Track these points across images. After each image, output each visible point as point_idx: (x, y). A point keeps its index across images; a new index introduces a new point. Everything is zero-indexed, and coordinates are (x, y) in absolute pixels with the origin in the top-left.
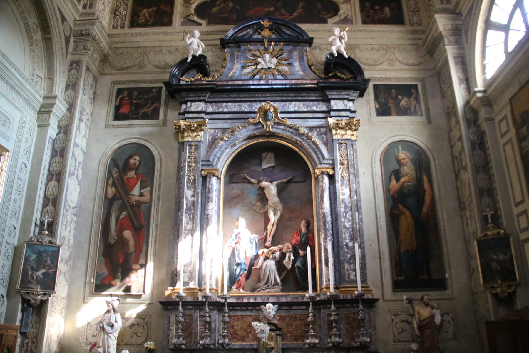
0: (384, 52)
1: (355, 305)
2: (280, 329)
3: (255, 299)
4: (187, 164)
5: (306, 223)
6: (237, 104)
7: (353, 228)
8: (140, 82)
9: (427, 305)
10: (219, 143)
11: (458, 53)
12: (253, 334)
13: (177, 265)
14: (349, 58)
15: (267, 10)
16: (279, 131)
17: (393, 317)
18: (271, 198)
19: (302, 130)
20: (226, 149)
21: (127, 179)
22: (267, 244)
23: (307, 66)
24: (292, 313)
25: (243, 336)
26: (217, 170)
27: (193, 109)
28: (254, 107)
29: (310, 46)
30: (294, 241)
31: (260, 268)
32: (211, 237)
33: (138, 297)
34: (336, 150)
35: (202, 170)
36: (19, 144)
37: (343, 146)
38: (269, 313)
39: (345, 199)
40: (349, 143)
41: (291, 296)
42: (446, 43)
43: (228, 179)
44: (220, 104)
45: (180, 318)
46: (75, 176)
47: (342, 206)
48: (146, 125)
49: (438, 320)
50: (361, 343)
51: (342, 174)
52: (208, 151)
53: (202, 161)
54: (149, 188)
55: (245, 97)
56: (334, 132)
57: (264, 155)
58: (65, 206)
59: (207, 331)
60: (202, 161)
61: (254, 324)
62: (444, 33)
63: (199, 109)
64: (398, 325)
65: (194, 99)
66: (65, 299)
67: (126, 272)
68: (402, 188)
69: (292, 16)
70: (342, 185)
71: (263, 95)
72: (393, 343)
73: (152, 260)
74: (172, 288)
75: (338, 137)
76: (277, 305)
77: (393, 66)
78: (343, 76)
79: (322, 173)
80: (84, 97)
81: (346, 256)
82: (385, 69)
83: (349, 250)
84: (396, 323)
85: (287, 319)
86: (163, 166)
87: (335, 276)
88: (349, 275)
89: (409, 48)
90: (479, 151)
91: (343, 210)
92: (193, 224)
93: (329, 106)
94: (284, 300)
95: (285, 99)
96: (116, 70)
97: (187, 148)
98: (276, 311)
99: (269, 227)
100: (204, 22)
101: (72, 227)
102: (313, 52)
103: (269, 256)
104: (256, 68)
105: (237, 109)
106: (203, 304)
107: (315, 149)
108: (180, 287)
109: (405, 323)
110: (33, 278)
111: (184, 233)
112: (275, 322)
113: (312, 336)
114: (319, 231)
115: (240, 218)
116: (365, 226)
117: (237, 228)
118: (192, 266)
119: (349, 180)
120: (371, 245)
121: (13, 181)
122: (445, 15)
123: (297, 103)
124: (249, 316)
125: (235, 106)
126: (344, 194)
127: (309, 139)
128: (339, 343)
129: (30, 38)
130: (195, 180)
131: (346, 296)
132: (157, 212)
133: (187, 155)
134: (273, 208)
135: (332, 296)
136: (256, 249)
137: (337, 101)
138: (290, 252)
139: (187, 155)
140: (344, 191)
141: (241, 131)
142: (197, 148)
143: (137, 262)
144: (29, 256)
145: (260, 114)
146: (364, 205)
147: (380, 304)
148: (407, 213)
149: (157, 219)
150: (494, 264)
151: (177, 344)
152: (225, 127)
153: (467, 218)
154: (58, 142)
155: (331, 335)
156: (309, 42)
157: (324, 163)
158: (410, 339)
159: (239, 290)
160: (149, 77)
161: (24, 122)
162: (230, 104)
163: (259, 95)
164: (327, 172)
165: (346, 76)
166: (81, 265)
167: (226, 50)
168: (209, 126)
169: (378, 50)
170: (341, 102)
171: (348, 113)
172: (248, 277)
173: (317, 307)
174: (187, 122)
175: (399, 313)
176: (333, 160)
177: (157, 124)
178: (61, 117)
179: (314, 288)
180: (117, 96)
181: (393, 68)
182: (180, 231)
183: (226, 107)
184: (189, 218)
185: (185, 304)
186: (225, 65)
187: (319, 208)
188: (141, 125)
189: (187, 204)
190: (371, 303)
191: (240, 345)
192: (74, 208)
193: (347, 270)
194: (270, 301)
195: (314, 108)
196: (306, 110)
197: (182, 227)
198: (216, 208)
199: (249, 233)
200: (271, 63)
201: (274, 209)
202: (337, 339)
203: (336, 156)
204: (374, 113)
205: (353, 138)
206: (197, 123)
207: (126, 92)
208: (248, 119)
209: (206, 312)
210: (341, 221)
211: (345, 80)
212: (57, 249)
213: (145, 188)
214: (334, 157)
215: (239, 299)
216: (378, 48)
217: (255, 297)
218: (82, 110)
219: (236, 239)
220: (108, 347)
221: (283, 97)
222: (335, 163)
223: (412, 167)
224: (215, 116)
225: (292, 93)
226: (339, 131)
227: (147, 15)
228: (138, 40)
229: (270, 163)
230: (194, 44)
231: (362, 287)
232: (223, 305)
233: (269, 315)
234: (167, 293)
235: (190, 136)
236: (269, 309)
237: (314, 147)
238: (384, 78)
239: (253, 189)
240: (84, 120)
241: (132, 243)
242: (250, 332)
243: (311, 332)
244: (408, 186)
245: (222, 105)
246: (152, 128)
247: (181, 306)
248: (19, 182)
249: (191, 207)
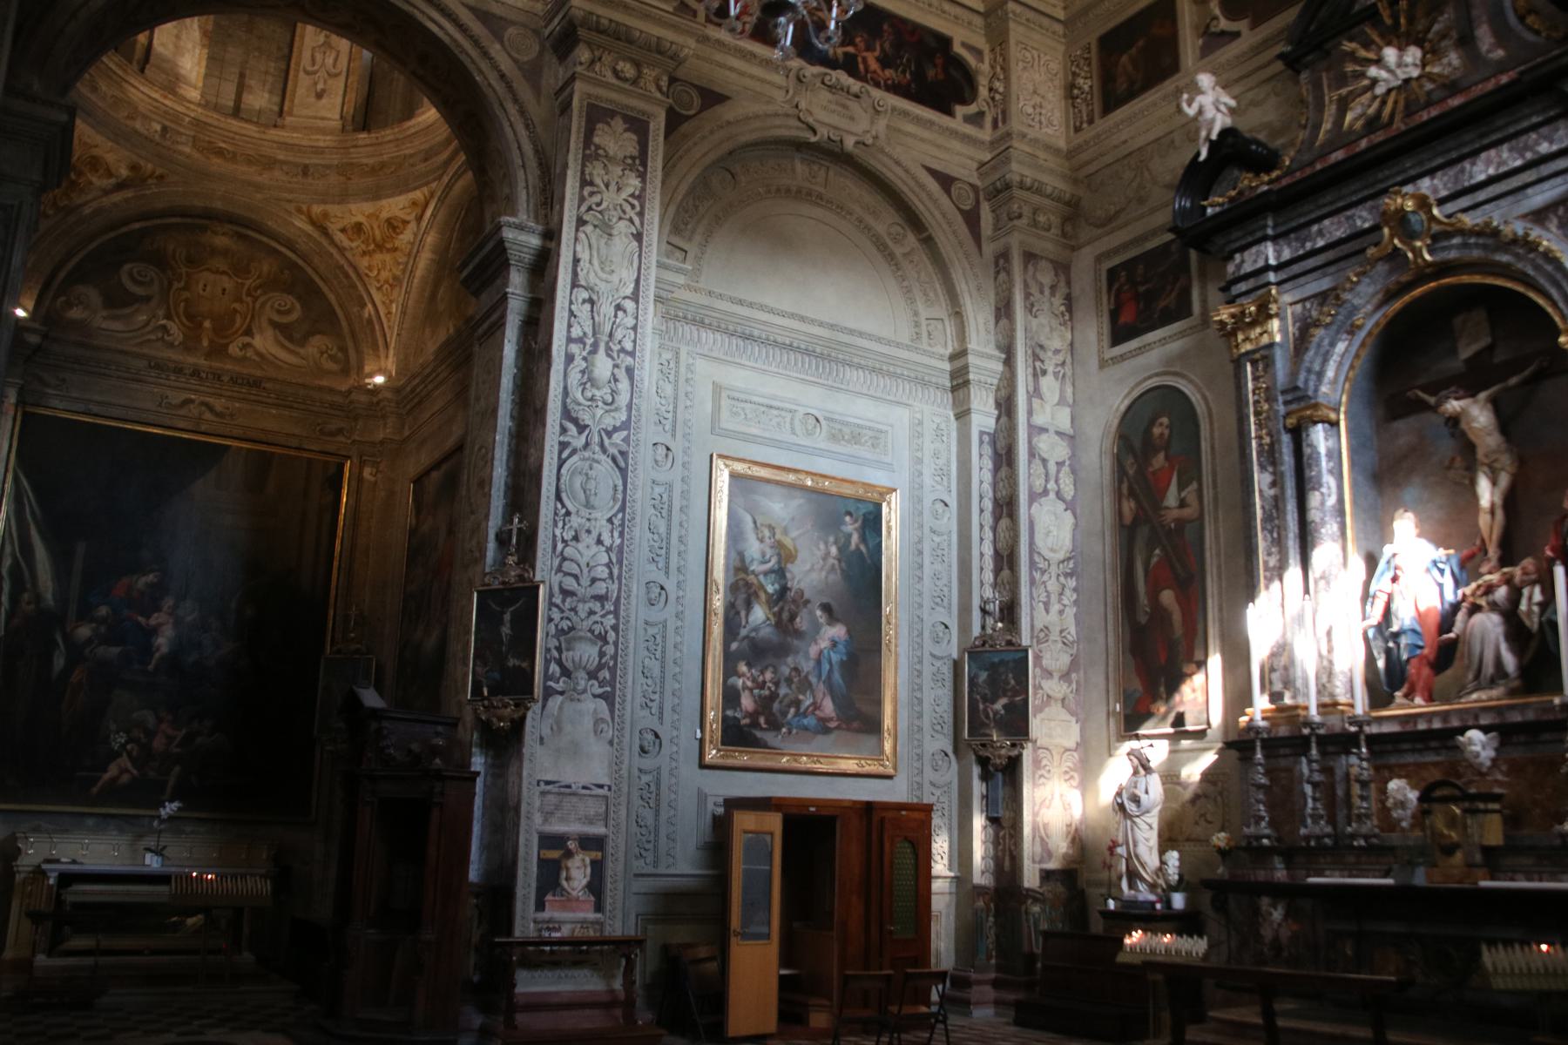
6: (1342, 217)
16: (1453, 255)
20: (1333, 344)
21: (1154, 473)
33: (1200, 734)
36: (919, 467)
38: (1477, 755)
44: (1304, 232)
46: (1052, 495)
54: (1194, 485)
55: (1355, 192)
58: (1032, 564)
60: (1284, 392)
65: (1243, 242)
66: (1075, 750)
67: (1174, 682)
73: (1218, 648)
80: (1035, 322)
92: (1280, 552)
94: (1516, 717)
95: (1454, 155)
96: (1098, 227)
98: (1496, 750)
100: (1242, 26)
101: (1066, 602)
107: (1554, 273)
110: (987, 716)
111: (1265, 577)
121: (920, 541)
123: (1493, 152)
125: (1339, 222)
129: (890, 257)
130: (1272, 445)
132: (1217, 537)
134: (1486, 469)
138: (1533, 583)
141: (1360, 288)
143: (1189, 658)
144: (976, 676)
149: (1218, 555)
154: (1001, 436)
159: (1412, 700)
161: (920, 423)
162: (1326, 222)
166: (1098, 678)
178: (995, 382)
183: (1320, 233)
185: (1323, 741)
188: (1163, 341)
189: (1263, 507)
192: (1063, 562)
195: (1544, 148)
196: (1518, 163)
200: (1406, 66)
207: (1123, 274)
208: (1363, 251)
212: (1020, 655)
213: (1187, 486)
217: (1445, 716)
218: (1038, 350)
219: (1388, 569)
220: (1135, 845)
221: (1449, 151)
224: (1296, 269)
227: (1130, 68)
228: (1123, 138)
237: (1549, 268)
240: (1050, 369)
241: (1177, 617)
246: (1184, 340)
247: (1259, 749)
248: (937, 539)
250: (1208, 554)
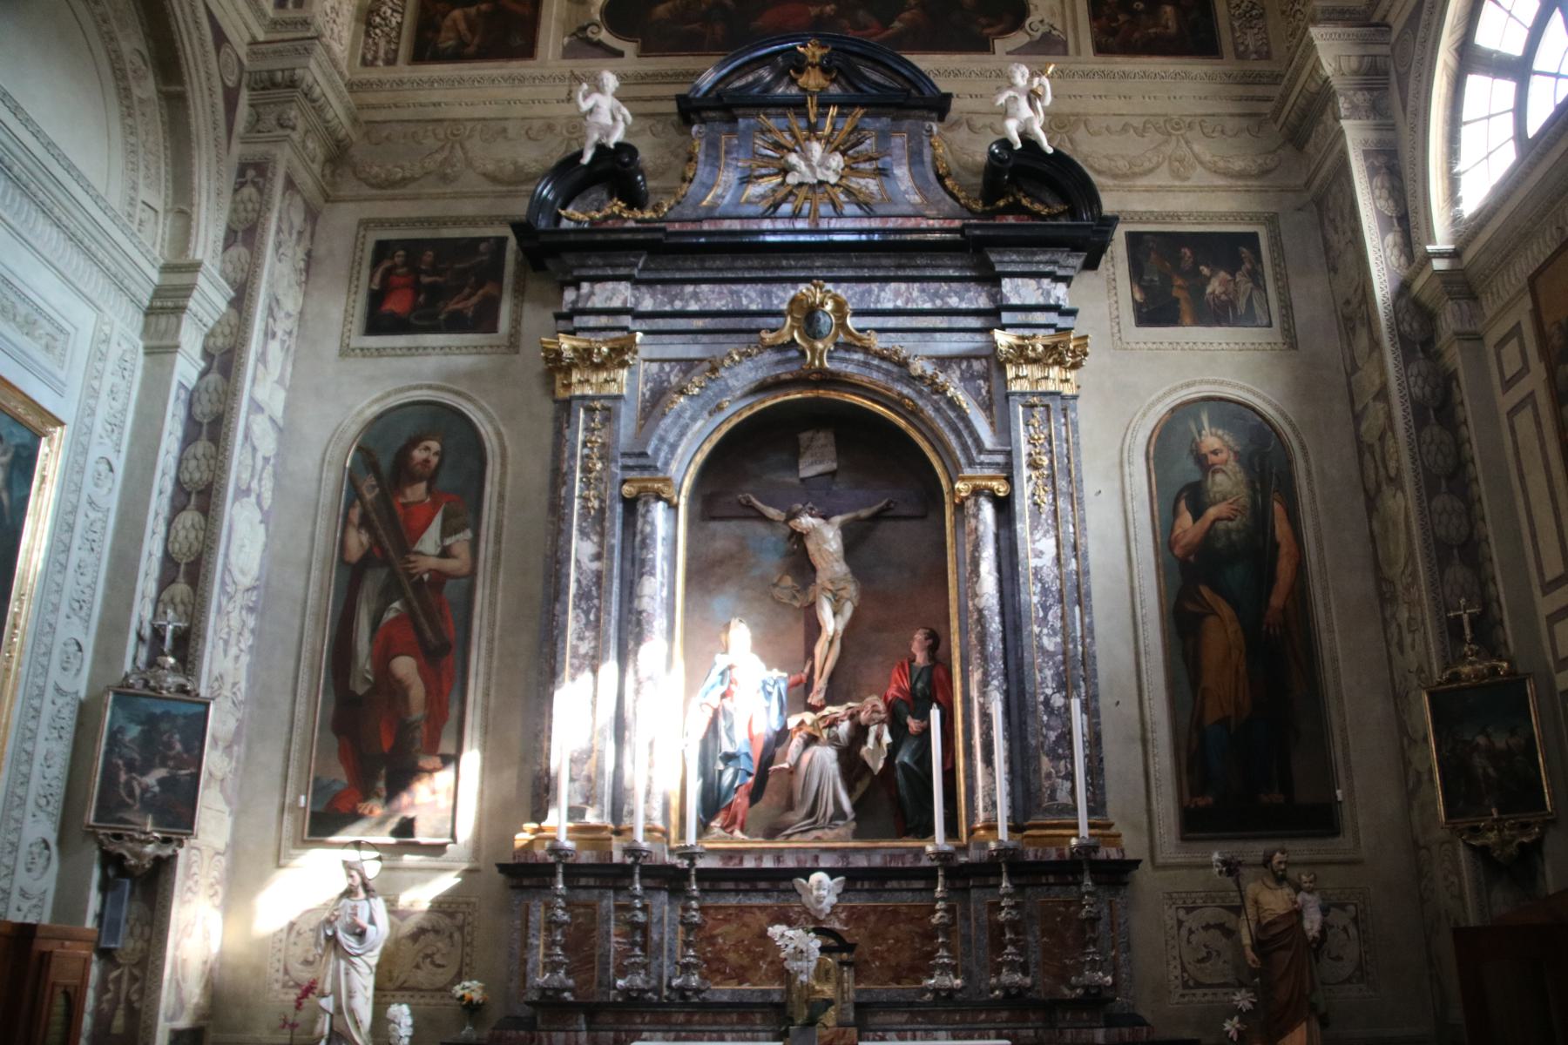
0: (1159, 137)
1: (1070, 878)
2: (850, 948)
3: (778, 859)
4: (579, 463)
5: (926, 639)
6: (725, 288)
7: (1064, 653)
8: (442, 222)
9: (1281, 879)
10: (672, 402)
11: (1380, 142)
12: (772, 962)
13: (548, 758)
15: (814, 11)
17: (1182, 913)
18: (824, 565)
19: (919, 366)
20: (694, 419)
21: (405, 506)
22: (814, 699)
23: (932, 176)
24: (886, 901)
25: (742, 967)
26: (666, 481)
27: (597, 302)
28: (777, 297)
29: (941, 119)
30: (892, 692)
31: (793, 770)
32: (650, 678)
33: (437, 850)
34: (1018, 425)
35: (624, 482)
36: (92, 402)
37: (1038, 413)
38: (819, 900)
39: (1041, 568)
40: (1055, 405)
41: (883, 851)
42: (1343, 112)
43: (698, 507)
44: (675, 289)
45: (560, 912)
46: (253, 499)
47: (1033, 589)
48: (458, 348)
49: (1312, 922)
50: (1087, 988)
51: (1034, 495)
52: (641, 427)
53: (624, 455)
54: (468, 534)
55: (750, 269)
56: (1011, 372)
57: (804, 437)
58: (223, 583)
59: (637, 951)
60: (624, 455)
61: (776, 931)
62: (1336, 83)
63: (616, 303)
64: (1194, 938)
65: (600, 272)
66: (223, 854)
67: (402, 777)
68: (1209, 535)
69: (890, 31)
70: (1033, 528)
71: (802, 263)
72: (1181, 991)
73: (476, 743)
74: (535, 826)
75: (1024, 386)
76: (841, 878)
77: (1188, 178)
78: (1037, 207)
79: (977, 492)
80: (278, 265)
81: (1046, 737)
82: (1160, 189)
83: (1054, 718)
84: (1191, 932)
85: (872, 918)
86: (509, 468)
87: (1012, 794)
88: (1053, 791)
89: (1231, 124)
90: (1436, 429)
91: (1035, 599)
92: (597, 638)
93: (997, 295)
94: (861, 862)
95: (866, 273)
96: (372, 186)
97: (578, 417)
98: (838, 895)
99: (820, 649)
100: (629, 48)
101: (243, 646)
102: (949, 135)
103: (818, 734)
104: (783, 183)
105: (727, 304)
106: (624, 871)
108: (557, 821)
109: (1218, 933)
110: (131, 794)
111: (572, 665)
112: (837, 926)
113: (945, 969)
114: (965, 661)
115: (735, 622)
116: (1099, 649)
117: (726, 651)
118: (593, 761)
119: (1055, 511)
120: (1118, 703)
121: (74, 511)
122: (1339, 30)
123: (903, 286)
124: (759, 908)
125: (721, 293)
126: (1039, 554)
127: (937, 392)
128: (1022, 990)
129: (125, 94)
130: (601, 511)
131: (1044, 852)
132: (492, 605)
133: (581, 437)
134: (830, 595)
135: (1003, 851)
136: (781, 713)
137: (1019, 281)
138: (882, 722)
140: (1039, 546)
141: (737, 369)
142: (609, 416)
143: (432, 747)
144: (121, 730)
145: (793, 317)
146: (1098, 586)
147: (1144, 877)
148: (1225, 609)
149: (492, 625)
150: (1478, 761)
151: (549, 989)
153: (1399, 626)
154: (205, 398)
155: (1001, 965)
156: (940, 105)
157: (981, 464)
158: (1230, 979)
159: (732, 832)
160: (468, 208)
161: (107, 340)
162: (705, 288)
163: (793, 263)
164: (992, 490)
165: (1048, 206)
166: (271, 756)
167: (695, 129)
168: (643, 352)
169: (1141, 132)
170: (1032, 283)
171: (1052, 318)
172: (756, 794)
173: (959, 884)
174: (580, 342)
175: (1199, 903)
176: (1009, 454)
177: (491, 347)
178: (211, 323)
179: (951, 829)
180: (375, 264)
181: (1186, 183)
182: (559, 659)
183: (695, 296)
184: (584, 621)
185: (574, 872)
186: (691, 175)
187: (966, 594)
188: (445, 350)
189: (578, 581)
190: (1116, 874)
191: (734, 992)
192: (248, 590)
193: (1049, 776)
194: (822, 865)
195: (954, 302)
196: (928, 306)
197: (564, 648)
198: (665, 593)
199: (762, 666)
200: (828, 168)
201: (835, 595)
202: (1018, 977)
203: (1018, 441)
204: (1128, 316)
205: (1067, 390)
206: (610, 345)
207: (401, 253)
208: (758, 331)
209: (636, 897)
210: (1031, 631)
211: (1043, 218)
212: (200, 709)
213: (456, 531)
214: (1010, 444)
215: (731, 858)
216: (1141, 126)
217: (778, 854)
218: (274, 304)
219: (722, 682)
220: (350, 996)
221: (862, 267)
222: (1015, 463)
223: (1241, 476)
224: (661, 324)
225: (888, 257)
226: (1026, 370)
227: (462, 26)
228: (435, 99)
229: (821, 462)
230: (600, 110)
231: (1091, 826)
232: (684, 874)
233: (820, 907)
234: (522, 838)
235: (587, 381)
236: (818, 889)
237: (952, 415)
238: (1160, 213)
239: (774, 539)
240: (280, 334)
241: (417, 692)
242: (763, 955)
243: (941, 957)
244: (1228, 532)
245: (682, 291)
246: (483, 357)
247: (560, 877)
248: (92, 515)
250: (476, 623)
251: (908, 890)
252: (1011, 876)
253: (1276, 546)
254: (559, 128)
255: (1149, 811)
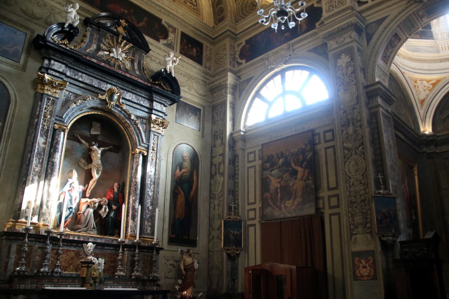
0: (187, 79)
4: (43, 114)
6: (90, 78)
9: (190, 256)
11: (232, 101)
14: (174, 77)
15: (122, 10)
17: (166, 261)
25: (66, 267)
27: (55, 68)
28: (102, 85)
41: (106, 239)
42: (228, 92)
44: (76, 72)
48: (5, 62)
49: (196, 266)
50: (153, 277)
53: (56, 116)
55: (98, 75)
56: (152, 125)
57: (94, 123)
60: (56, 116)
62: (229, 86)
63: (61, 70)
64: (168, 267)
65: (58, 59)
68: (182, 175)
69: (138, 25)
71: (111, 79)
72: (164, 279)
76: (95, 245)
77: (190, 91)
78: (165, 87)
79: (140, 152)
81: (147, 216)
84: (167, 266)
86: (17, 108)
88: (147, 229)
89: (201, 82)
90: (232, 166)
91: (149, 182)
93: (152, 104)
94: (99, 241)
95: (125, 88)
99: (91, 182)
103: (90, 205)
105: (89, 82)
106: (45, 238)
109: (172, 266)
111: (33, 174)
113: (121, 270)
122: (233, 75)
123: (132, 94)
124: (72, 251)
126: (151, 172)
127: (135, 125)
130: (48, 130)
133: (45, 106)
137: (157, 103)
139: (45, 106)
142: (54, 103)
150: (231, 236)
152: (78, 93)
153: (215, 205)
156: (147, 50)
158: (173, 277)
162: (84, 75)
163: (109, 78)
164: (143, 153)
165: (167, 88)
167: (88, 28)
168: (68, 88)
169: (184, 76)
170: (160, 105)
175: (170, 259)
176: (149, 145)
177: (16, 67)
183: (81, 76)
184: (38, 161)
189: (38, 149)
195: (142, 103)
196: (136, 102)
197: (31, 168)
201: (97, 169)
211: (165, 90)
214: (149, 143)
215: (66, 236)
217: (79, 237)
223: (189, 164)
225: (131, 86)
226: (155, 126)
229: (96, 131)
232: (58, 240)
235: (50, 90)
236: (91, 247)
244: (185, 176)
249: (41, 153)
251: (109, 249)
252: (138, 249)
253: (193, 181)
254: (48, 7)
255: (162, 237)
